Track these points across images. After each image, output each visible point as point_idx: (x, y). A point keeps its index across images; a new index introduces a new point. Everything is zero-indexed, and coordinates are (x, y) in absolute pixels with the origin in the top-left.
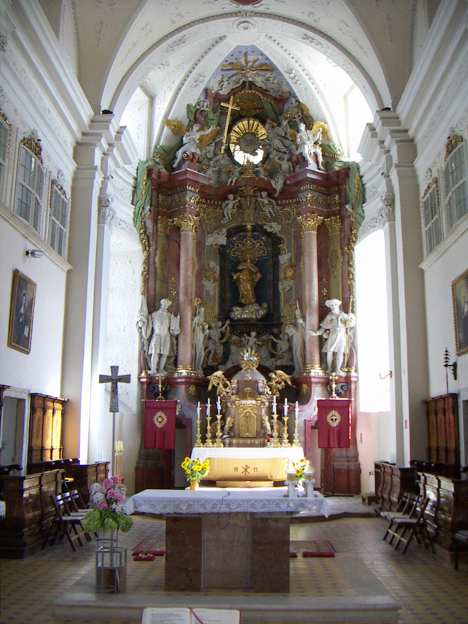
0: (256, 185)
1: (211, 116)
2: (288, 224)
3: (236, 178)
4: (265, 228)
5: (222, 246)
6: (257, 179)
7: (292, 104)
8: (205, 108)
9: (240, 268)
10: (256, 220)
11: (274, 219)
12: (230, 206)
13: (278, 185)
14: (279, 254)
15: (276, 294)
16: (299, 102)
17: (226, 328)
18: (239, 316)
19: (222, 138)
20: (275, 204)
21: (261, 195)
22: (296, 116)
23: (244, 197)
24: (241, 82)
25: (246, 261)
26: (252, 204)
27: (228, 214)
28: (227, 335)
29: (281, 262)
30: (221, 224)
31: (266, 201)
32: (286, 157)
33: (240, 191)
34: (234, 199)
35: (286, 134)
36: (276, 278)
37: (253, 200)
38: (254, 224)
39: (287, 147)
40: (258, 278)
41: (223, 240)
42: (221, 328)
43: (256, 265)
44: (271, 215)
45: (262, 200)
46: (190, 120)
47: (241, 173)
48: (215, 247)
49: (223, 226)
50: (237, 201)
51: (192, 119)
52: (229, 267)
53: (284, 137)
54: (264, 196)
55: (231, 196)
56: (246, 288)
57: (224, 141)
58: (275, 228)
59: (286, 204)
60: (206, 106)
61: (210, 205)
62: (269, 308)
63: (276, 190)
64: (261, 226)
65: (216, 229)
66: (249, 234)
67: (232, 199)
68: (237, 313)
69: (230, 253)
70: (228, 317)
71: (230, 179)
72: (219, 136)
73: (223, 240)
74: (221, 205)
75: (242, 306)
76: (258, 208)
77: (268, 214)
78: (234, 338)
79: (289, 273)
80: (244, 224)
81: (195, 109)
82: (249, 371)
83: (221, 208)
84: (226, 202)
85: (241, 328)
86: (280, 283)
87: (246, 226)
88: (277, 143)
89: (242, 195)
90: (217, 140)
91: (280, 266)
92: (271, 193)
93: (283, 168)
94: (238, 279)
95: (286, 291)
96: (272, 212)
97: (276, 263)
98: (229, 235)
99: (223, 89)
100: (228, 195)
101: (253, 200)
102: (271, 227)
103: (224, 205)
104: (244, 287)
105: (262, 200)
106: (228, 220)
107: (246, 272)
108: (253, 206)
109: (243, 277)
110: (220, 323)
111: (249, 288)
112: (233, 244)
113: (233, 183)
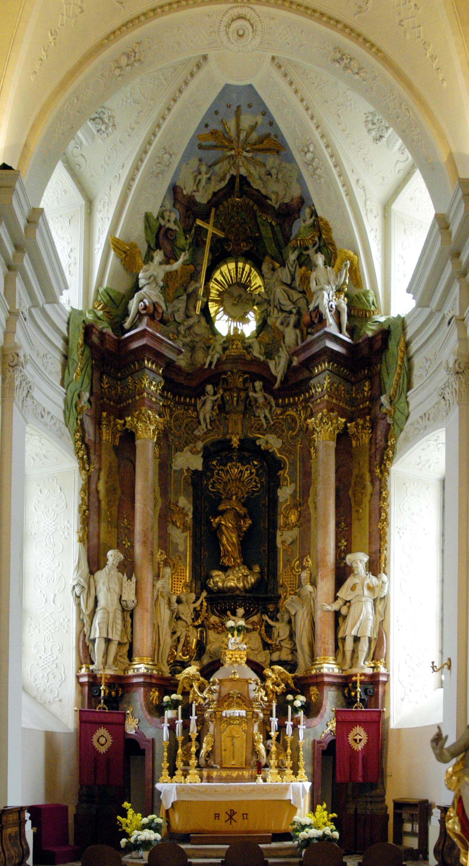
0: (246, 369)
1: (182, 242)
2: (292, 438)
3: (216, 356)
4: (258, 443)
7: (304, 221)
8: (172, 226)
10: (245, 431)
19: (198, 285)
20: (273, 404)
22: (310, 244)
23: (230, 390)
24: (228, 177)
26: (240, 402)
27: (205, 419)
32: (293, 319)
35: (293, 279)
37: (243, 394)
39: (294, 303)
45: (255, 395)
46: (149, 246)
47: (225, 349)
50: (219, 395)
51: (153, 245)
53: (290, 286)
55: (209, 388)
57: (201, 292)
59: (290, 405)
63: (276, 378)
64: (253, 441)
67: (212, 392)
71: (209, 358)
72: (193, 282)
80: (228, 437)
81: (157, 225)
82: (236, 665)
87: (230, 440)
88: (280, 293)
90: (190, 290)
93: (287, 339)
96: (269, 416)
99: (201, 189)
101: (243, 394)
102: (267, 443)
108: (241, 408)
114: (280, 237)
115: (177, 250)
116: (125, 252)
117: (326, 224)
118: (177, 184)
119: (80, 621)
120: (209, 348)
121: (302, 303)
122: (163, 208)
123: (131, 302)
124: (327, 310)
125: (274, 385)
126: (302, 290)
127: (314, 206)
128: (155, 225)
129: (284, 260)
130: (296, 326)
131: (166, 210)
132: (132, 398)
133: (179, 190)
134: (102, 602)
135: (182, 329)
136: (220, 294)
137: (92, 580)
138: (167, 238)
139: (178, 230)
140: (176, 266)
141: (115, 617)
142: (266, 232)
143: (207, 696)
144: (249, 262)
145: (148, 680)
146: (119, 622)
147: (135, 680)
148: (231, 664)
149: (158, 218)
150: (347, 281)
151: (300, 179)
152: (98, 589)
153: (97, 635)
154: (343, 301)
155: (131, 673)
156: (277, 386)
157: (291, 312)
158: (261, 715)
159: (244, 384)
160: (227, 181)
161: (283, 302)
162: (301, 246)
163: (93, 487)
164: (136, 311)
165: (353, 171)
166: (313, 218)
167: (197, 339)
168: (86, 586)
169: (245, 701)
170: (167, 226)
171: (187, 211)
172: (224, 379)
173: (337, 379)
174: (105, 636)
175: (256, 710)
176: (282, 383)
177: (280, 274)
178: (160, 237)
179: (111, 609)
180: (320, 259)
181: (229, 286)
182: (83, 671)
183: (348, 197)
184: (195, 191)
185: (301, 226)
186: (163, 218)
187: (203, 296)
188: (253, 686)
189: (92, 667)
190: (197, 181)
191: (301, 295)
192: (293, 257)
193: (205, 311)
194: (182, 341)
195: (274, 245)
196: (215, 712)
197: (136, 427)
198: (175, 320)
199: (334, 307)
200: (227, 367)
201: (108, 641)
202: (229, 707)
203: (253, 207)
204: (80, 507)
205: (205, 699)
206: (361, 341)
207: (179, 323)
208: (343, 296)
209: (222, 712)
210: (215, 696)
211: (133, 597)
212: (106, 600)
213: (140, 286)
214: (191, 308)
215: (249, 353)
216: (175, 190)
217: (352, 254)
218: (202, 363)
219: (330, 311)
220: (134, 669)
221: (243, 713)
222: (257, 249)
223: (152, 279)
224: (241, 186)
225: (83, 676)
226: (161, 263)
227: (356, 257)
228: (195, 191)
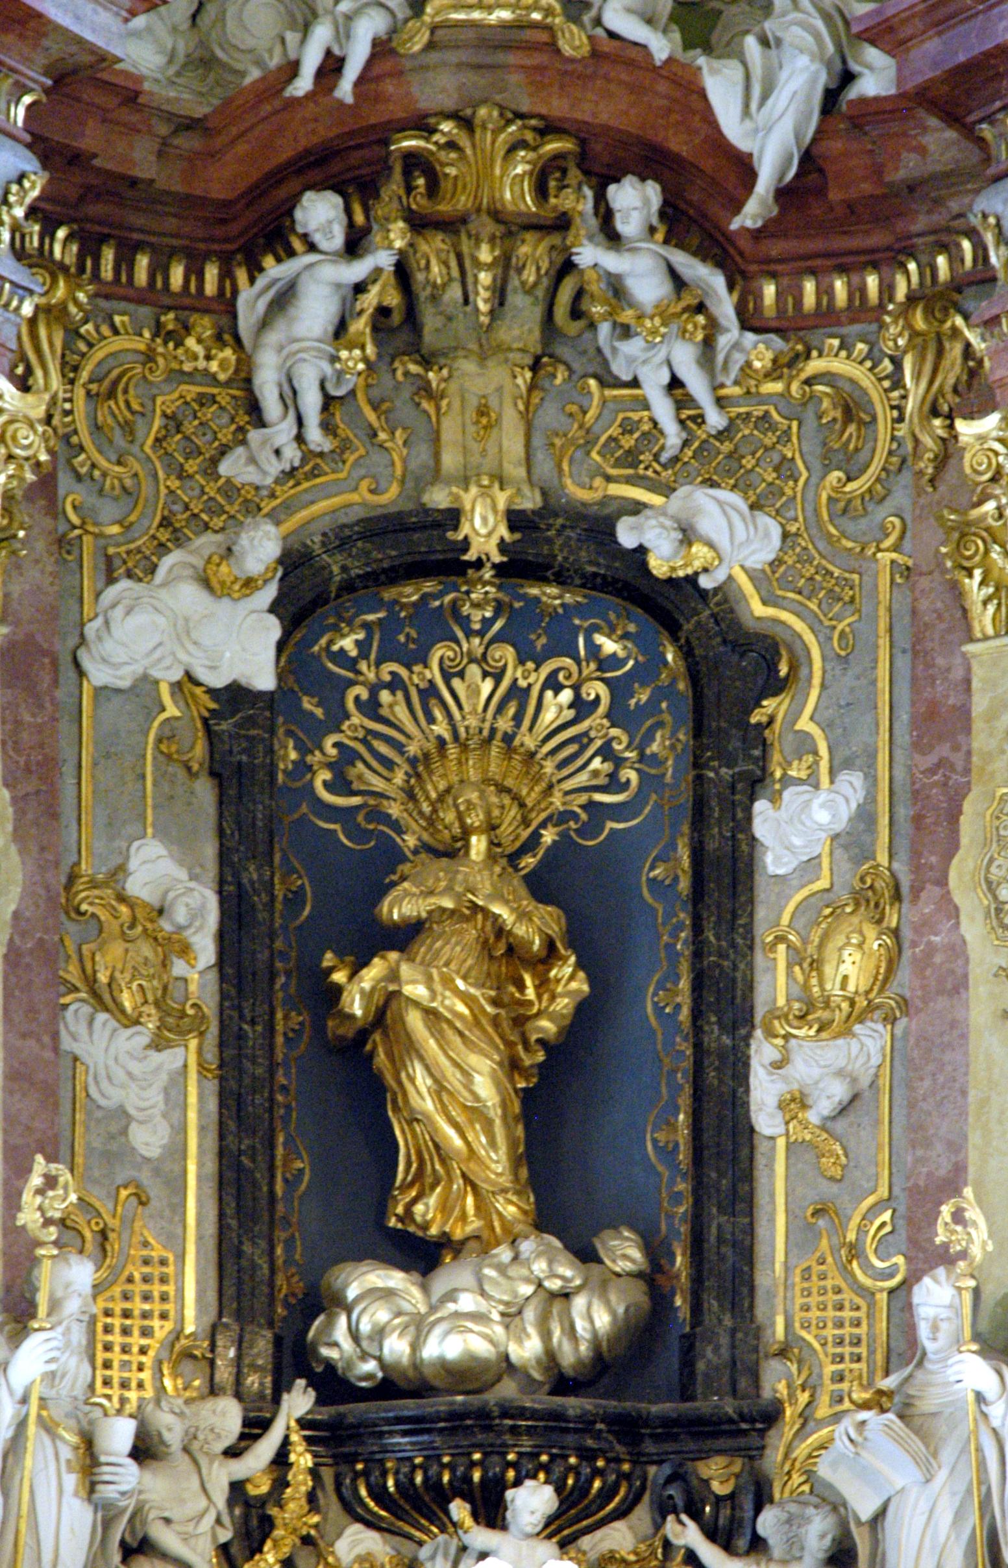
0: (557, 107)
2: (843, 509)
3: (369, 28)
4: (627, 537)
5: (235, 696)
6: (573, 42)
9: (400, 907)
10: (544, 466)
11: (716, 459)
12: (315, 311)
14: (756, 783)
15: (723, 1147)
17: (281, 1460)
18: (397, 1347)
20: (725, 306)
21: (606, 216)
23: (451, 226)
25: (451, 851)
26: (516, 299)
27: (290, 396)
28: (292, 1512)
29: (775, 861)
30: (230, 489)
31: (647, 286)
33: (414, 162)
34: (354, 246)
36: (723, 1004)
37: (533, 252)
38: (530, 502)
40: (563, 1005)
42: (233, 1453)
43: (540, 887)
45: (612, 262)
48: (172, 711)
49: (248, 504)
50: (384, 259)
52: (295, 899)
54: (629, 225)
55: (320, 213)
56: (456, 1091)
59: (827, 316)
61: (119, 291)
62: (653, 1276)
63: (743, 168)
64: (598, 526)
65: (179, 540)
66: (482, 593)
67: (338, 240)
68: (381, 1319)
69: (303, 768)
70: (296, 1359)
74: (226, 305)
75: (422, 1255)
76: (570, 318)
77: (663, 409)
79: (851, 966)
80: (438, 498)
83: (228, 333)
84: (275, 270)
86: (762, 1052)
87: (454, 516)
89: (419, 202)
91: (764, 892)
92: (699, 194)
94: (386, 1009)
95: (813, 1117)
96: (697, 385)
97: (724, 878)
98: (304, 598)
100: (293, 201)
101: (533, 252)
102: (687, 535)
103: (251, 302)
104: (440, 1089)
105: (612, 262)
106: (292, 454)
107: (456, 948)
108: (522, 327)
109: (434, 989)
110: (228, 1416)
111: (485, 1089)
112: (332, 692)
113: (352, 72)
125: (737, 206)
156: (753, 212)
159: (541, 192)
176: (784, 194)
200: (437, 89)
218: (275, 61)
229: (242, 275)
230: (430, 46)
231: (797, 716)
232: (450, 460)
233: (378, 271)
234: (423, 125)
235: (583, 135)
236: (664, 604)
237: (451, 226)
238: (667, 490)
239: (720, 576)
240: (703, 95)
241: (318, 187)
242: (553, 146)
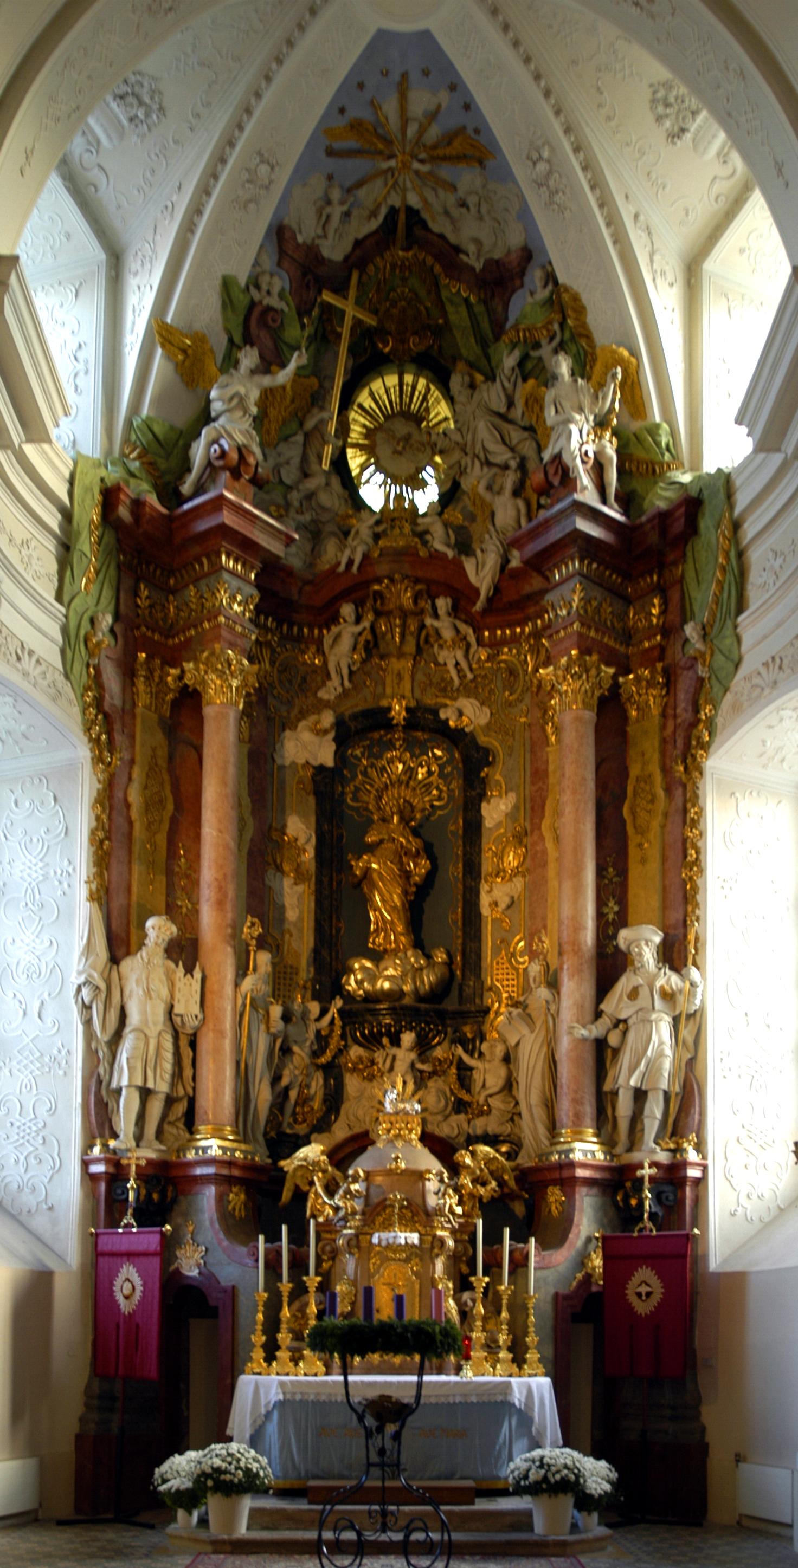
0: (420, 574)
1: (293, 332)
6: (423, 553)
7: (532, 294)
8: (274, 302)
11: (469, 689)
12: (346, 643)
13: (481, 573)
16: (556, 283)
19: (325, 415)
20: (472, 639)
23: (388, 614)
24: (383, 211)
31: (448, 634)
32: (510, 480)
35: (510, 404)
38: (413, 704)
39: (512, 450)
41: (326, 755)
44: (462, 677)
46: (231, 341)
47: (377, 537)
50: (366, 624)
51: (237, 339)
54: (442, 611)
55: (347, 610)
57: (332, 428)
58: (468, 714)
59: (504, 642)
60: (277, 290)
63: (477, 592)
71: (347, 552)
72: (315, 410)
73: (326, 755)
77: (453, 673)
78: (356, 1052)
80: (384, 703)
82: (399, 1144)
84: (335, 629)
85: (369, 1022)
87: (389, 709)
88: (484, 433)
90: (310, 424)
97: (473, 829)
98: (344, 735)
99: (331, 233)
106: (340, 690)
108: (410, 647)
114: (485, 325)
115: (285, 348)
116: (184, 352)
117: (576, 298)
118: (286, 222)
119: (91, 1054)
120: (346, 534)
121: (528, 449)
122: (258, 269)
123: (194, 445)
124: (578, 461)
125: (474, 604)
126: (527, 424)
127: (550, 263)
128: (242, 301)
129: (492, 370)
130: (516, 493)
131: (263, 273)
132: (195, 627)
133: (287, 235)
134: (134, 1017)
135: (295, 497)
136: (369, 434)
137: (115, 974)
138: (266, 325)
139: (286, 309)
140: (283, 376)
141: (159, 1047)
142: (458, 316)
143: (341, 1204)
144: (425, 372)
145: (225, 1172)
146: (168, 1056)
147: (199, 1171)
148: (390, 1141)
149: (247, 288)
150: (617, 406)
151: (525, 215)
152: (127, 992)
153: (125, 1082)
154: (608, 445)
155: (191, 1156)
156: (479, 606)
157: (506, 467)
158: (450, 1243)
159: (415, 603)
160: (381, 218)
161: (491, 446)
162: (525, 341)
163: (119, 794)
164: (206, 462)
165: (627, 197)
166: (550, 287)
167: (325, 517)
168: (103, 986)
169: (418, 1214)
170: (265, 302)
171: (304, 275)
172: (376, 592)
173: (597, 593)
174: (139, 1082)
175: (440, 1233)
176: (489, 600)
177: (485, 395)
178: (252, 325)
179: (153, 1032)
180: (564, 366)
181: (387, 417)
182: (97, 1151)
183: (618, 246)
184: (319, 237)
185: (525, 305)
186: (258, 287)
187: (336, 436)
188: (432, 1185)
189: (112, 1143)
190: (324, 218)
191: (526, 434)
192: (510, 361)
193: (340, 463)
194: (294, 520)
195: (473, 340)
196: (357, 1236)
197: (204, 682)
198: (281, 482)
199: (591, 454)
201: (145, 1093)
202: (387, 1226)
203: (432, 268)
204: (93, 833)
205: (337, 1209)
206: (644, 519)
207: (289, 488)
208: (608, 435)
209: (371, 1235)
210: (358, 1205)
211: (196, 1009)
212: (143, 1012)
213: (213, 414)
214: (313, 458)
215: (425, 543)
216: (280, 234)
217: (626, 353)
218: (334, 562)
219: (583, 462)
220: (197, 1149)
221: (414, 1238)
222: (440, 348)
223: (235, 401)
224: (409, 228)
225: (97, 1161)
226: (253, 372)
227: (633, 360)
228: (319, 237)
229: (325, 632)
230: (380, 555)
231: (496, 775)
232: (389, 691)
233: (364, 629)
234: (379, 581)
235: (429, 583)
236: (455, 738)
237: (388, 614)
238: (455, 699)
239: (472, 727)
240: (464, 569)
241: (347, 602)
242: (419, 587)
